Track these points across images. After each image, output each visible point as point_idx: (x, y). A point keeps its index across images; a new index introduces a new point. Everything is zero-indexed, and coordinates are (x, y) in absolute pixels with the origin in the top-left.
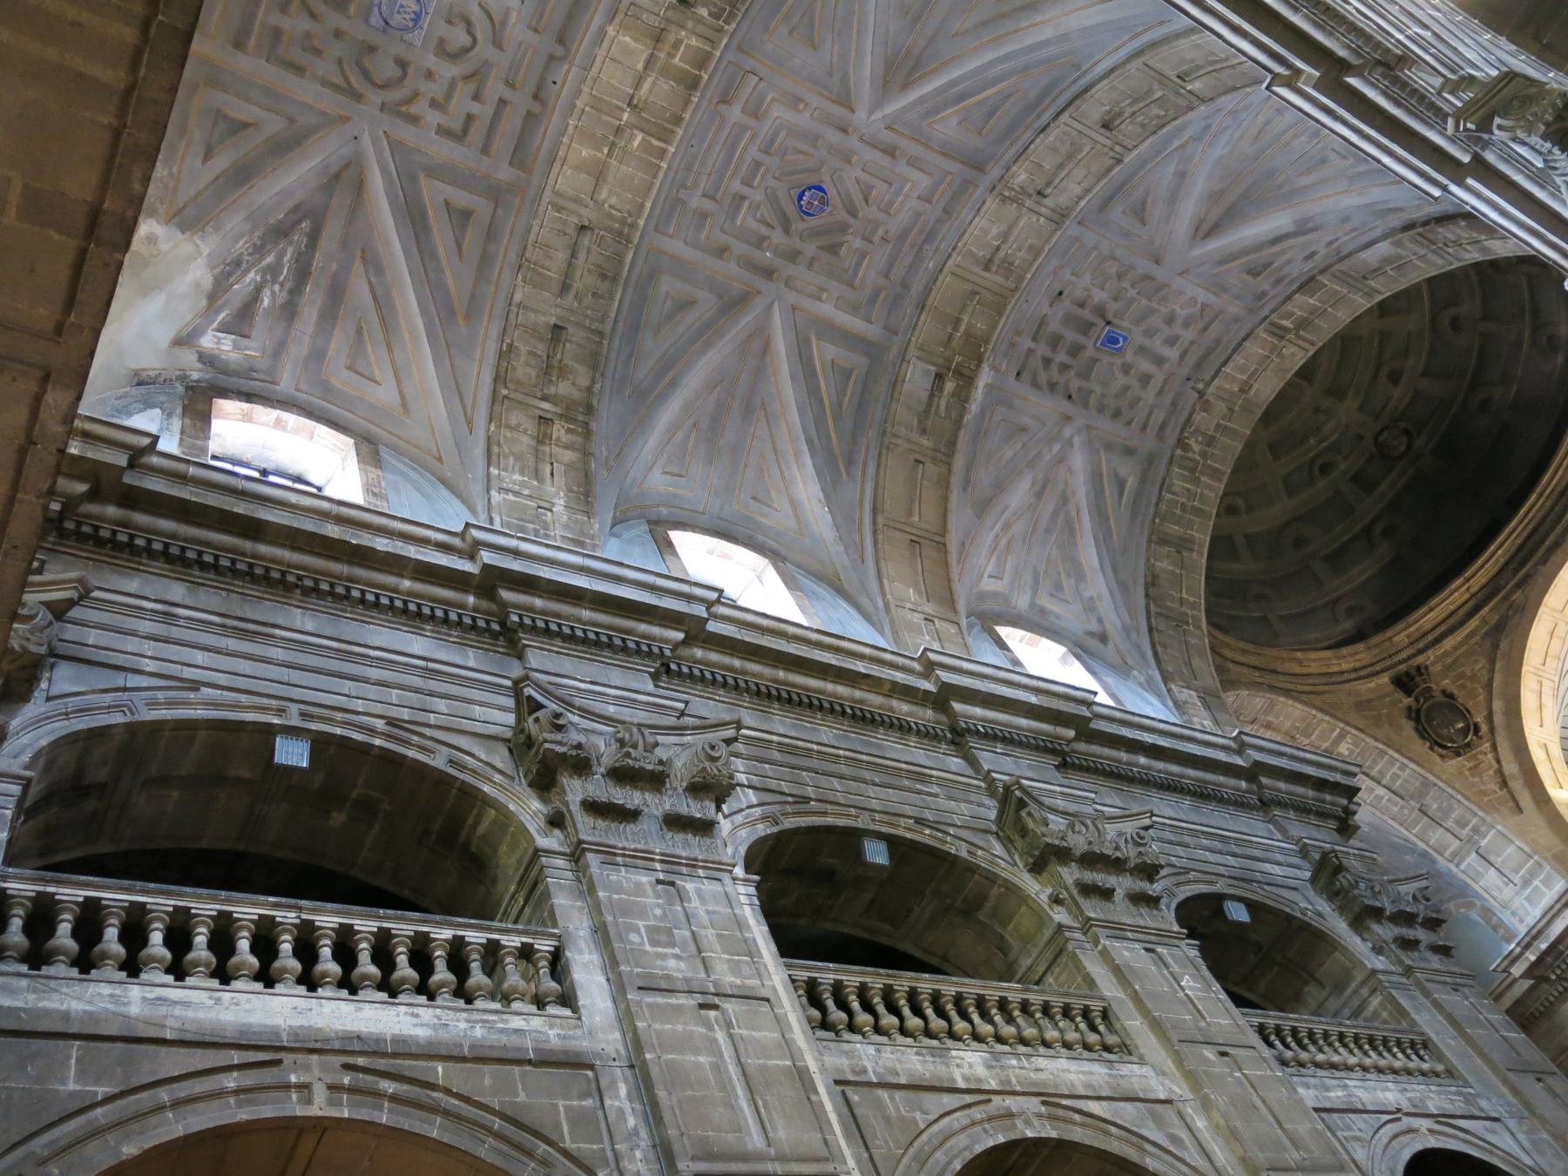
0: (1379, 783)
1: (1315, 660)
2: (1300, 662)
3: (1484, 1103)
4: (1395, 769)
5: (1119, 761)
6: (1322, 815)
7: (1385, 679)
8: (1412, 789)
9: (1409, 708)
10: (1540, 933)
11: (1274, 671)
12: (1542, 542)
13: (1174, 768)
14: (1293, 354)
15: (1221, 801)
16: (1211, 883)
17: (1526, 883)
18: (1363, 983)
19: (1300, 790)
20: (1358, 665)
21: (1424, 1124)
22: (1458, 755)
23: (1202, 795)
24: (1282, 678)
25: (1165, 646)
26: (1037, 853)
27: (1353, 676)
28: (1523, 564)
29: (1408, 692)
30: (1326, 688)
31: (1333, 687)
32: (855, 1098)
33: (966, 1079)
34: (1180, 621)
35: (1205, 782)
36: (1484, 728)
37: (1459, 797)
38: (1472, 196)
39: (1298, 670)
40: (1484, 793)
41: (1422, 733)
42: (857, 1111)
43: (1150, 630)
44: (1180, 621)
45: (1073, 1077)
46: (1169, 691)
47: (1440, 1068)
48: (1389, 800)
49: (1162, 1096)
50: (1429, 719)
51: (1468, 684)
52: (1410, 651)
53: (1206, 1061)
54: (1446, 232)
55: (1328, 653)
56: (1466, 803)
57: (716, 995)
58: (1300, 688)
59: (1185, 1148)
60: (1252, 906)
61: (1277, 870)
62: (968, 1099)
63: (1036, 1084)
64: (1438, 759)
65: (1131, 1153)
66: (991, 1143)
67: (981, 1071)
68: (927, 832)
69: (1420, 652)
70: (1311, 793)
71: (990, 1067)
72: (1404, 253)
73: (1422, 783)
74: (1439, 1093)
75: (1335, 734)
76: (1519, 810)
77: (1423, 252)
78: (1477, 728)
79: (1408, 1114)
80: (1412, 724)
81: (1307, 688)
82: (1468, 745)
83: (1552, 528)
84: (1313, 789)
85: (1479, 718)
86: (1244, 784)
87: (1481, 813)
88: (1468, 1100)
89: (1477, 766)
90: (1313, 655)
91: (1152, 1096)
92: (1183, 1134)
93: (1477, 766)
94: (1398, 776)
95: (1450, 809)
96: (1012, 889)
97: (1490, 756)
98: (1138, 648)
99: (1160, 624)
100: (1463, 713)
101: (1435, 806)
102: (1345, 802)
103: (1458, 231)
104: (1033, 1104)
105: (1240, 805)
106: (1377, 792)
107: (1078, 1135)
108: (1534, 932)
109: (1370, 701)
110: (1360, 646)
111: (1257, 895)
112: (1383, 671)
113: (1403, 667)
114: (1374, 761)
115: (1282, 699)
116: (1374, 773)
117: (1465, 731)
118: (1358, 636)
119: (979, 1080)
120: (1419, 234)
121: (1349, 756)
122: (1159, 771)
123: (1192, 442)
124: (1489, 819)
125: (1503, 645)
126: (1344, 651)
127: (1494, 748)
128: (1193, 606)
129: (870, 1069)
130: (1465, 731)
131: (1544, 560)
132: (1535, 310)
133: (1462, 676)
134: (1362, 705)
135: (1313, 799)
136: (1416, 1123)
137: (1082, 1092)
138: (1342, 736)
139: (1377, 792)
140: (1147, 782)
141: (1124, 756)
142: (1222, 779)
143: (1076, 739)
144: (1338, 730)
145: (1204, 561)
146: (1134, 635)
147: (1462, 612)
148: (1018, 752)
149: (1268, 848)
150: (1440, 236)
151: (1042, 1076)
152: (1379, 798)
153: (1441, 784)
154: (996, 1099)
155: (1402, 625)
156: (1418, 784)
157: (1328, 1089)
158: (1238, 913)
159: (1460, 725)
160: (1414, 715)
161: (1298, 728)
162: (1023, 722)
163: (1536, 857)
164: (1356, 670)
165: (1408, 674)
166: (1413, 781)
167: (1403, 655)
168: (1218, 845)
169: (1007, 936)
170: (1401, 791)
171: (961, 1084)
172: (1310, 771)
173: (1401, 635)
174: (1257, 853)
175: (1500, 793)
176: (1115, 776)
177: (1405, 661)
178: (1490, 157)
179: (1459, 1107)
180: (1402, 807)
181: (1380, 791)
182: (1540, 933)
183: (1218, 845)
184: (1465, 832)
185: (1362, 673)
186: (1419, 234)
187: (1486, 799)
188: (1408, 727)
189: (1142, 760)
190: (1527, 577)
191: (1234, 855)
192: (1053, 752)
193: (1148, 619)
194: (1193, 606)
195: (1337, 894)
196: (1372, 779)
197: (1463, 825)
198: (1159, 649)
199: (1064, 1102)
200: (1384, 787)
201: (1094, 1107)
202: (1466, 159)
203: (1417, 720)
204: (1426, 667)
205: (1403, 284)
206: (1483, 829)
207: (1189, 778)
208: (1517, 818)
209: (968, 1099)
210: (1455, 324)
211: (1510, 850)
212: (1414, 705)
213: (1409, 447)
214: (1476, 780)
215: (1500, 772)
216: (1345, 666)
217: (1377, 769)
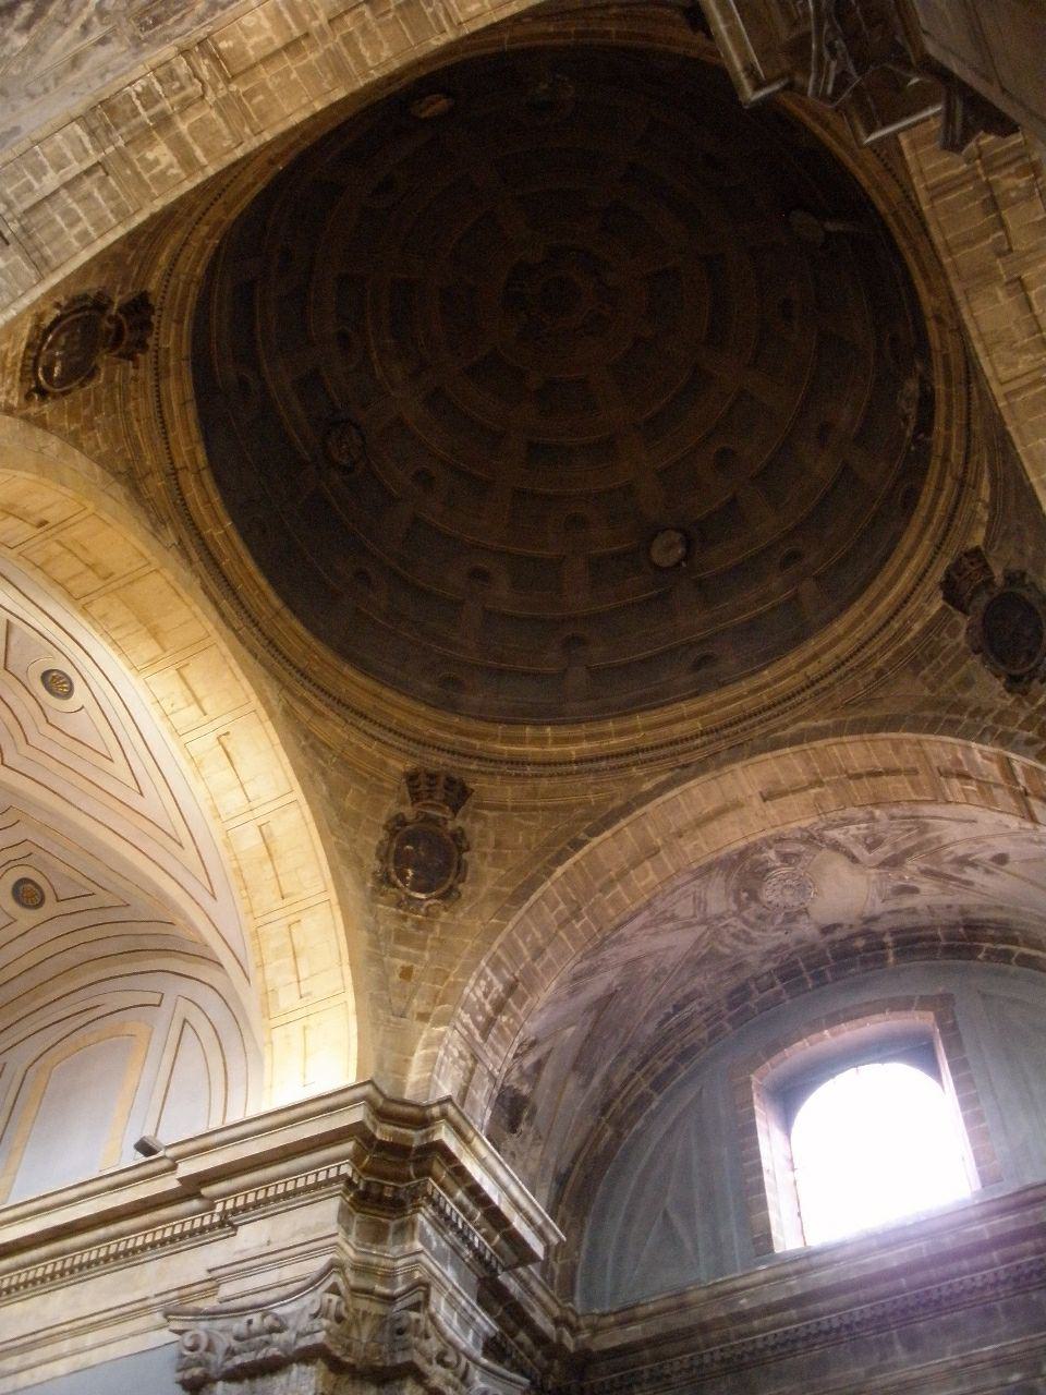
0: (67, 185)
1: (254, 184)
4: (85, 224)
8: (40, 237)
14: (1014, 364)
48: (30, 188)
51: (86, 412)
73: (46, 260)
75: (199, 153)
94: (71, 225)
106: (51, 173)
114: (113, 197)
116: (88, 185)
121: (142, 159)
123: (1022, 182)
131: (205, 590)
138: (188, 162)
139: (51, 173)
144: (203, 160)
152: (39, 171)
155: (186, 350)
156: (48, 251)
159: (57, 370)
161: (250, 95)
166: (56, 245)
170: (38, 217)
180: (9, 205)
181: (51, 181)
190: (191, 562)
196: (78, 178)
200: (55, 192)
217: (96, 194)
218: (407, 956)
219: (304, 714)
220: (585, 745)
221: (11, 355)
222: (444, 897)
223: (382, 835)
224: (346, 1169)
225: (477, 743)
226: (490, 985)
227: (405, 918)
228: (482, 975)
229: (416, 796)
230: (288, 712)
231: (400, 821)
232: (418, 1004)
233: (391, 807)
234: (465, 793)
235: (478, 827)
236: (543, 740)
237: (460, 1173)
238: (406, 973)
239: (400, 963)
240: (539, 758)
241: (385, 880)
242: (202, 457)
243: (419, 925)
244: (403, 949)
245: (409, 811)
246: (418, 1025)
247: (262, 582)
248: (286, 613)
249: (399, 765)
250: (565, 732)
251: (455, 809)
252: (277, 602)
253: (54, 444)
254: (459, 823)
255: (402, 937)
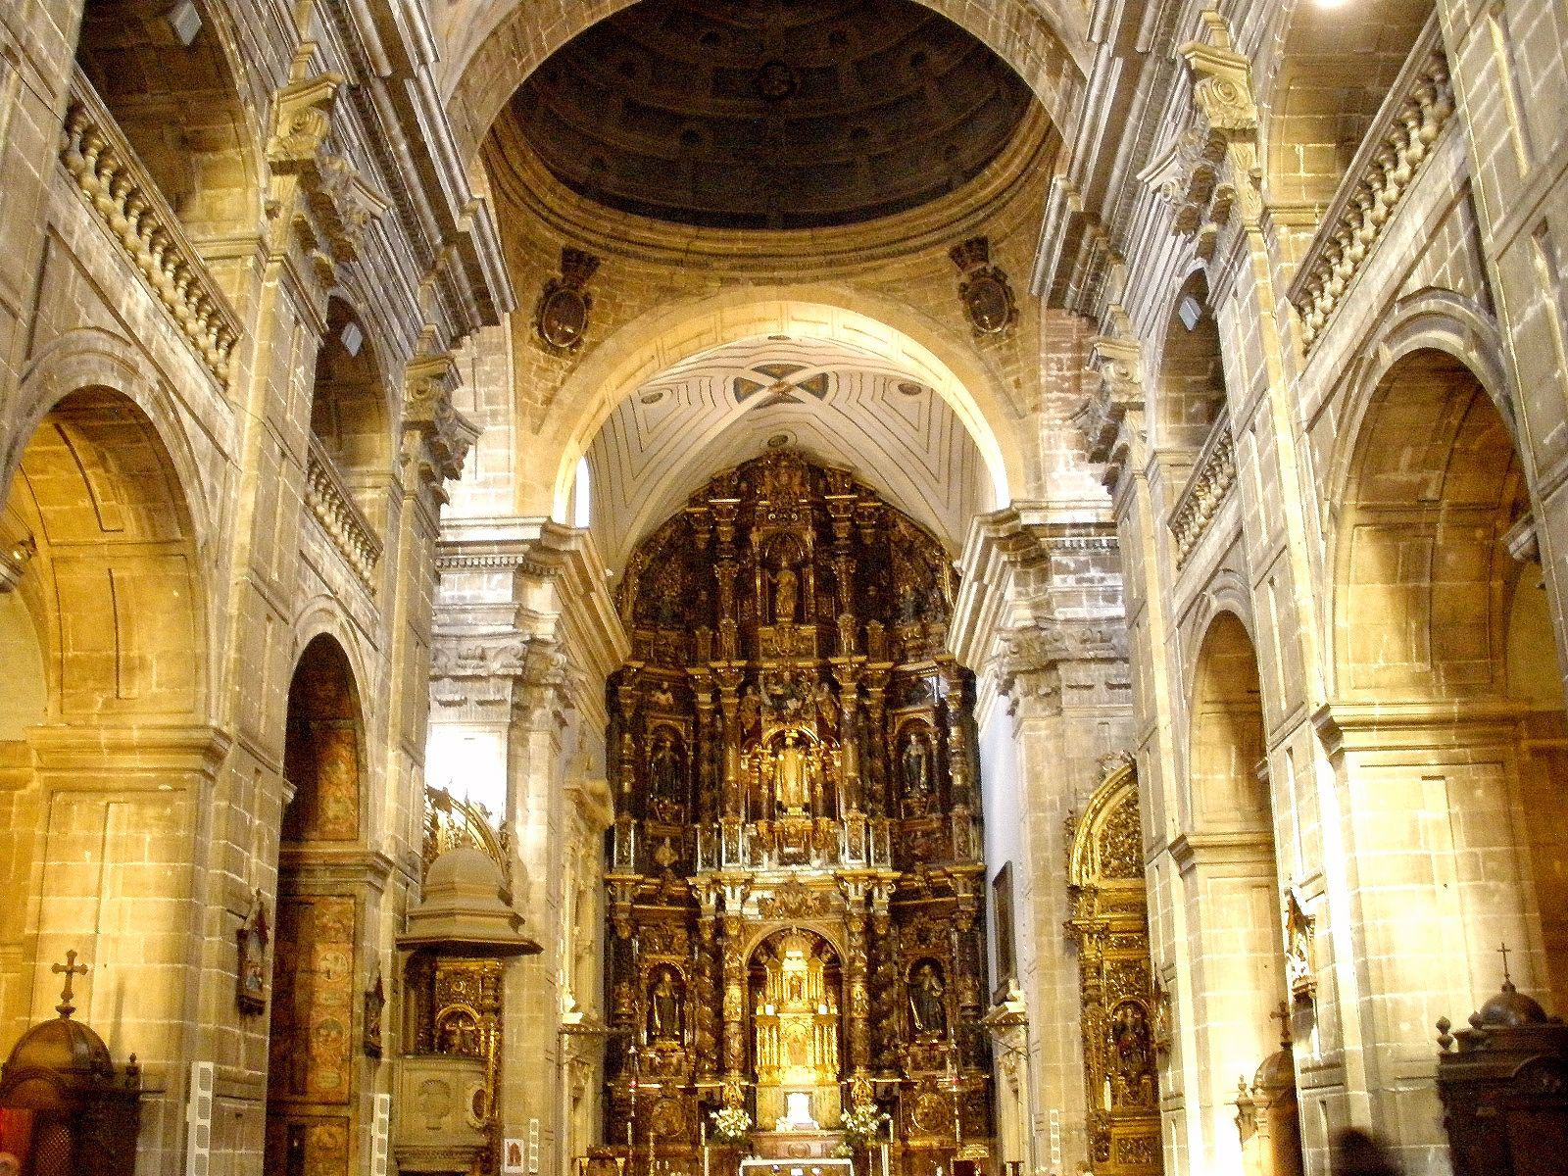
2: (524, 161)
3: (378, 632)
5: (388, 128)
6: (457, 318)
7: (562, 242)
9: (554, 280)
10: (458, 527)
11: (500, 148)
12: (774, 269)
13: (414, 178)
15: (413, 237)
16: (357, 298)
17: (485, 484)
18: (376, 474)
19: (465, 284)
20: (557, 209)
21: (342, 617)
22: (544, 349)
23: (408, 218)
24: (499, 157)
25: (488, 58)
26: (295, 158)
27: (545, 213)
28: (742, 268)
29: (565, 269)
30: (518, 201)
31: (523, 206)
32: (53, 253)
33: (129, 312)
34: (518, 51)
35: (419, 209)
36: (582, 350)
37: (511, 380)
38: (1101, 70)
39: (516, 166)
40: (529, 395)
41: (541, 309)
42: (49, 267)
43: (494, 33)
44: (518, 51)
45: (188, 379)
46: (453, 98)
47: (371, 583)
49: (227, 449)
50: (554, 304)
52: (601, 240)
53: (273, 450)
54: (1034, 34)
55: (549, 178)
56: (511, 389)
57: (23, 49)
58: (503, 181)
59: (214, 505)
60: (366, 348)
61: (398, 330)
62: (120, 331)
63: (163, 359)
64: (527, 337)
65: (183, 475)
66: (111, 385)
67: (140, 315)
68: (233, 46)
69: (607, 248)
70: (469, 294)
71: (147, 317)
72: (993, 7)
74: (363, 602)
76: (536, 430)
77: (1003, 23)
78: (577, 344)
79: (338, 601)
80: (542, 294)
81: (507, 187)
82: (558, 351)
83: (790, 268)
84: (474, 293)
85: (586, 339)
86: (439, 240)
87: (512, 406)
88: (374, 622)
89: (547, 370)
90: (538, 166)
91: (221, 444)
92: (219, 492)
93: (547, 370)
95: (495, 381)
96: (248, 163)
97: (562, 373)
98: (470, 34)
99: (505, 38)
100: (580, 324)
101: (487, 368)
102: (479, 322)
103: (1040, 45)
104: (151, 377)
105: (420, 254)
107: (163, 429)
108: (453, 523)
109: (533, 244)
110: (574, 198)
111: (377, 341)
112: (567, 233)
113: (582, 247)
115: (485, 177)
117: (567, 337)
118: (580, 189)
119: (135, 320)
120: (1020, 12)
122: (403, 168)
124: (512, 415)
125: (664, 308)
126: (562, 189)
127: (572, 370)
128: (540, 50)
129: (76, 236)
130: (567, 337)
131: (758, 283)
132: (970, 119)
133: (612, 298)
134: (526, 243)
135: (465, 301)
136: (338, 611)
137: (186, 397)
140: (387, 167)
141: (396, 130)
142: (432, 219)
143: (384, 80)
145: (587, 25)
146: (478, 22)
147: (665, 255)
148: (338, 43)
149: (408, 308)
150: (1026, 30)
151: (170, 356)
153: (510, 358)
154: (134, 348)
156: (495, 340)
157: (313, 539)
158: (352, 339)
159: (570, 330)
160: (551, 289)
162: (369, 23)
163: (512, 474)
164: (551, 211)
165: (580, 255)
167: (592, 237)
168: (384, 274)
169: (198, 200)
171: (123, 313)
172: (488, 277)
173: (608, 221)
174: (399, 304)
175: (539, 405)
176: (374, 137)
177: (589, 242)
178: (1149, 65)
179: (364, 621)
182: (458, 527)
183: (384, 274)
184: (485, 408)
185: (553, 218)
186: (1020, 12)
187: (525, 400)
188: (536, 294)
189: (403, 147)
190: (736, 280)
191: (386, 290)
192: (360, 73)
193: (503, 22)
194: (540, 50)
195: (420, 392)
197: (490, 399)
198: (483, 56)
199: (171, 394)
201: (187, 419)
202: (1139, 49)
203: (548, 294)
204: (598, 264)
205: (961, 22)
206: (500, 419)
207: (414, 196)
208: (529, 433)
209: (120, 331)
210: (918, 59)
211: (502, 452)
212: (559, 282)
213: (782, 97)
214: (536, 379)
215: (555, 389)
216: (549, 199)
218: (1013, 372)
219: (869, 278)
220: (1017, 161)
221: (542, 364)
222: (1010, 320)
223: (961, 304)
224: (1004, 558)
225: (971, 201)
226: (1059, 361)
227: (1000, 348)
228: (1048, 361)
229: (963, 266)
230: (860, 288)
231: (964, 287)
232: (1029, 402)
233: (955, 282)
234: (982, 242)
235: (1003, 257)
236: (996, 175)
237: (1057, 528)
238: (1018, 384)
239: (1011, 379)
240: (1005, 184)
241: (977, 334)
242: (690, 230)
243: (1010, 347)
244: (1009, 369)
245: (965, 278)
246: (1034, 416)
247: (788, 234)
248: (817, 232)
249: (943, 253)
250: (1003, 160)
251: (985, 259)
252: (807, 233)
253: (610, 344)
254: (993, 263)
255: (1005, 362)
